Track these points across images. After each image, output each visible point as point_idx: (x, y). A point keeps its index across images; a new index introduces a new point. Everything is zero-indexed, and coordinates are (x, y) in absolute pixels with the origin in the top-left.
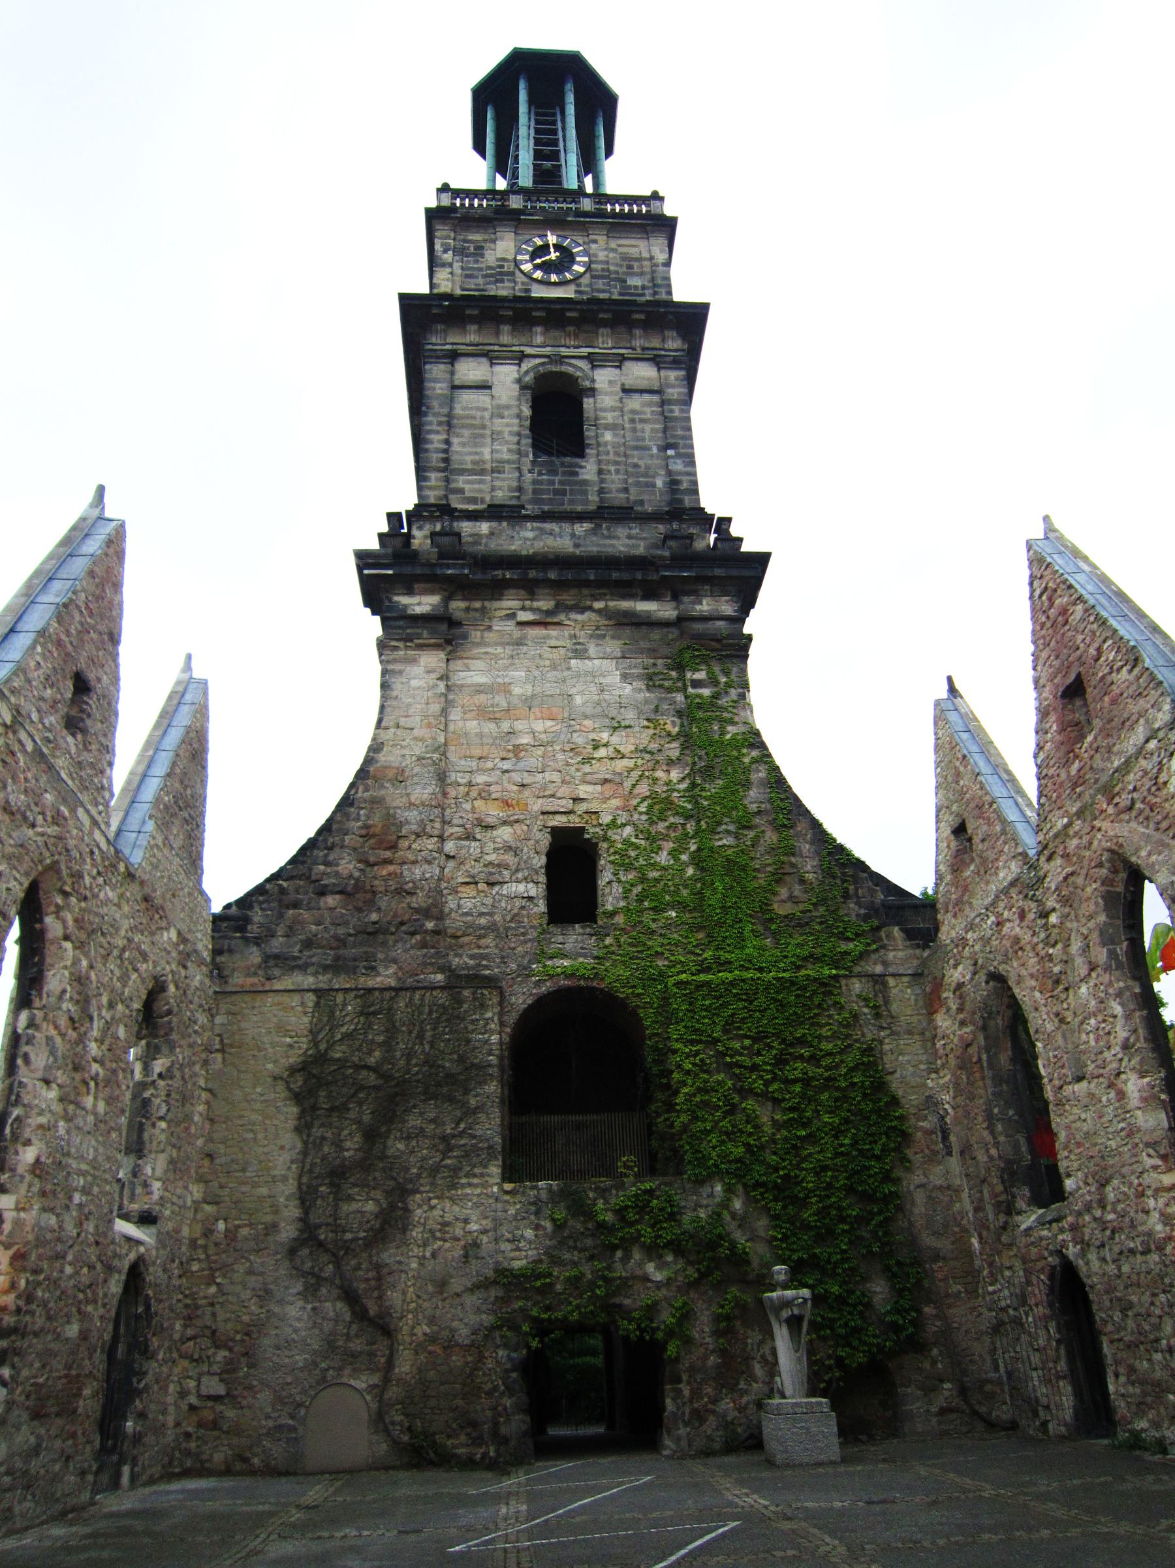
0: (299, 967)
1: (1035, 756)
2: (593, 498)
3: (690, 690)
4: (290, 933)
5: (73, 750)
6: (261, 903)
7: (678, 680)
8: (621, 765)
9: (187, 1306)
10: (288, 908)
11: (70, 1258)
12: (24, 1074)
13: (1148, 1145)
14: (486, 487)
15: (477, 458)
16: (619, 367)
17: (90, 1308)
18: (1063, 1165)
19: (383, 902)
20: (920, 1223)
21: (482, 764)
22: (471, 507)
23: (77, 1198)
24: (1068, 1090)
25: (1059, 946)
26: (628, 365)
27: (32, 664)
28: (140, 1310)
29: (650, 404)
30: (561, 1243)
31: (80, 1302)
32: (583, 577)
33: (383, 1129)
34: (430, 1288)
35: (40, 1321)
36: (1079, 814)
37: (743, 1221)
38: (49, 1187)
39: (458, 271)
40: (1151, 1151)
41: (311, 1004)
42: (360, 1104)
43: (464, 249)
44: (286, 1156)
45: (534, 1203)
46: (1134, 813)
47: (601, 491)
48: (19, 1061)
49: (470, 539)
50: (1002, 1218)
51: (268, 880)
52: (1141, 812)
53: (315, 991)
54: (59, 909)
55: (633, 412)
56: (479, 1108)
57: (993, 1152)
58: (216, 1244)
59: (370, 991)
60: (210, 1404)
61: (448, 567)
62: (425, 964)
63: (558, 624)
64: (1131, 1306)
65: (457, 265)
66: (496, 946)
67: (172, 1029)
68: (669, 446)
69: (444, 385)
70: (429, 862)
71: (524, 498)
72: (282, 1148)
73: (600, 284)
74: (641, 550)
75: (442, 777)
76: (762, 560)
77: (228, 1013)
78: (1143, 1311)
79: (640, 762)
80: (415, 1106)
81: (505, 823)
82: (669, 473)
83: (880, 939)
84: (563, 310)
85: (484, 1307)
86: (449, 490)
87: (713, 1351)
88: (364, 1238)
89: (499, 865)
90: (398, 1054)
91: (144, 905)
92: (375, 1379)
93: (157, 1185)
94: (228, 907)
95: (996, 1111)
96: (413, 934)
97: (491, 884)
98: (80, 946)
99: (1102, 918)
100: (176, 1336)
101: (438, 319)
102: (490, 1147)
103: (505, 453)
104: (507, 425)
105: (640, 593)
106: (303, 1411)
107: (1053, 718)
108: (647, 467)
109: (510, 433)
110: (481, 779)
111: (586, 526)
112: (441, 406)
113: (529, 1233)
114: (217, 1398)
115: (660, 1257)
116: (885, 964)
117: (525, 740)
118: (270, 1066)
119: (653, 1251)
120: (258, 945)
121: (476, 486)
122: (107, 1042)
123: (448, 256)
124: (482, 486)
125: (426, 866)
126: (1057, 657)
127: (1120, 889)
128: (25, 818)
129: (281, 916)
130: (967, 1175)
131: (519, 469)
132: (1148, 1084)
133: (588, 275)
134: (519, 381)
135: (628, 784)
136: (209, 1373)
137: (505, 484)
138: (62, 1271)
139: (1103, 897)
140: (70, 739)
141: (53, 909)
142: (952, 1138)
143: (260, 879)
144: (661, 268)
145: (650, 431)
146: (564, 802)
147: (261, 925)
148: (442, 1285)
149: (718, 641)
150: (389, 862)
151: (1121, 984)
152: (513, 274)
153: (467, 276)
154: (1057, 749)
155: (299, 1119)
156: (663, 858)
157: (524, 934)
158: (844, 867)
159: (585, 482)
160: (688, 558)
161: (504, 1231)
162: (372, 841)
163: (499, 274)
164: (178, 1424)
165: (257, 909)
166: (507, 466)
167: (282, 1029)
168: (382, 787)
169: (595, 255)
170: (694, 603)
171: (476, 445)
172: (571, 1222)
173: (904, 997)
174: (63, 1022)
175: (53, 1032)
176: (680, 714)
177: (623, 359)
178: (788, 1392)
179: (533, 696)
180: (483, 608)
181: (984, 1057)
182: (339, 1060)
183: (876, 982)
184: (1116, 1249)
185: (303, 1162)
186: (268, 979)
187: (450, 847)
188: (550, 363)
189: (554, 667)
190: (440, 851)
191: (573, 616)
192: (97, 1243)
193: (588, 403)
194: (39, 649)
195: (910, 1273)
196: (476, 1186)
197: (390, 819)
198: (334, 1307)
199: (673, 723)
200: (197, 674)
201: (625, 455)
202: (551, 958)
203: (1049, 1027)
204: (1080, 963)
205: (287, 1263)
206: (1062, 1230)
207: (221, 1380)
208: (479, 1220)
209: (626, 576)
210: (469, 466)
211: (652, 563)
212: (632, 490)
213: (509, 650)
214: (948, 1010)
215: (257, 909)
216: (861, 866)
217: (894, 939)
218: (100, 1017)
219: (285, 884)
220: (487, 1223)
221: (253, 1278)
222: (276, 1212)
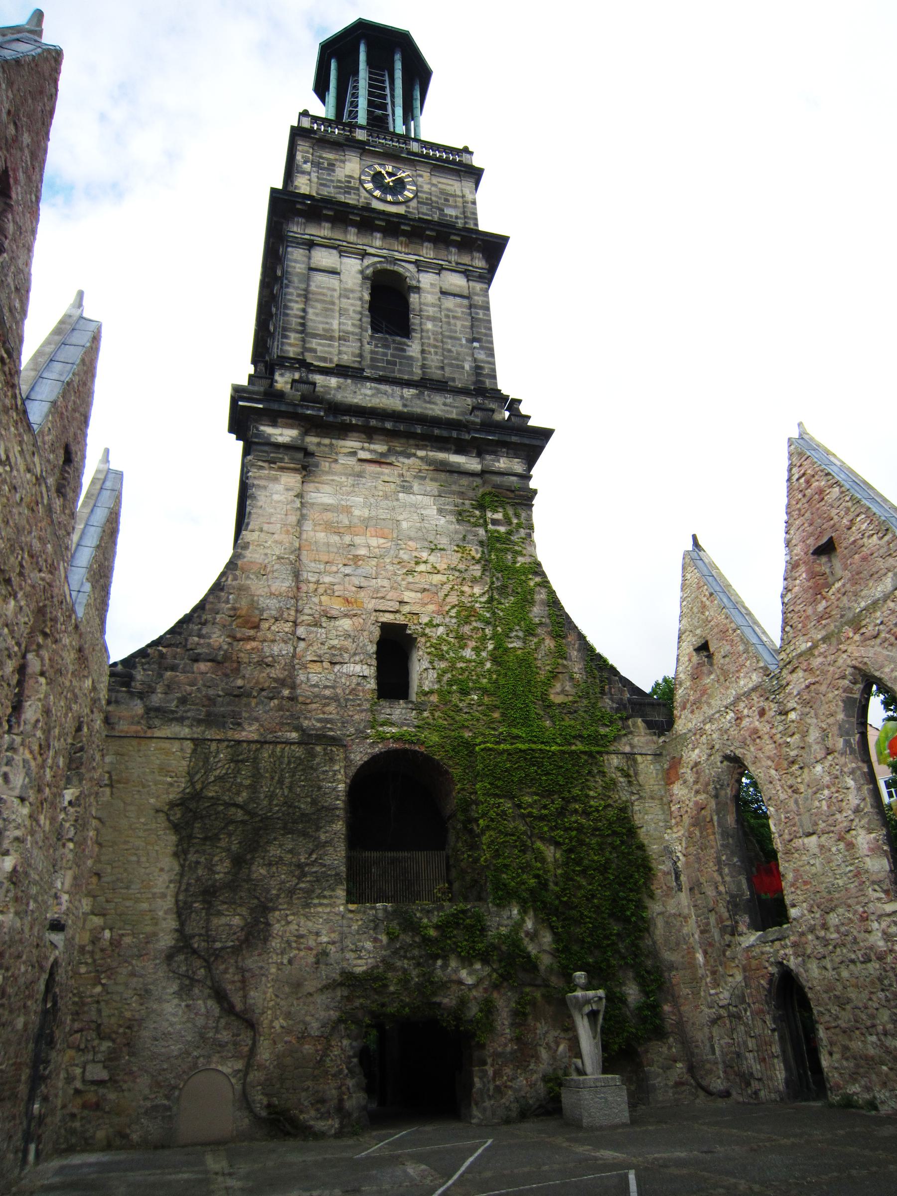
1: (782, 596)
3: (490, 527)
4: (169, 688)
6: (143, 664)
7: (481, 517)
8: (437, 579)
9: (74, 1003)
10: (166, 669)
13: (874, 883)
14: (335, 351)
15: (327, 326)
16: (439, 274)
18: (788, 899)
19: (247, 671)
20: (660, 940)
21: (328, 568)
24: (798, 843)
25: (796, 736)
26: (445, 274)
29: (461, 306)
30: (395, 952)
32: (412, 430)
33: (249, 856)
34: (287, 989)
36: (824, 639)
37: (533, 936)
39: (315, 180)
40: (876, 887)
41: (189, 751)
42: (230, 835)
43: (319, 163)
44: (165, 877)
45: (373, 921)
46: (878, 641)
47: (423, 366)
50: (727, 937)
51: (149, 646)
52: (886, 640)
53: (192, 739)
54: (39, 646)
55: (448, 310)
56: (328, 843)
57: (722, 888)
58: (102, 950)
59: (239, 742)
61: (308, 408)
62: (282, 724)
63: (390, 464)
64: (849, 1001)
65: (314, 175)
66: (338, 713)
67: (82, 764)
68: (474, 340)
69: (303, 266)
70: (285, 642)
72: (162, 870)
73: (424, 209)
74: (453, 415)
75: (297, 575)
76: (545, 434)
77: (117, 754)
78: (861, 1005)
79: (451, 577)
80: (275, 839)
82: (475, 360)
83: (628, 727)
84: (400, 224)
85: (333, 1005)
87: (511, 1040)
88: (232, 947)
89: (340, 649)
90: (262, 796)
92: (239, 1065)
93: (65, 897)
95: (724, 858)
96: (271, 699)
97: (333, 664)
99: (841, 716)
100: (67, 1029)
101: (300, 213)
102: (337, 874)
104: (352, 305)
105: (453, 448)
106: (177, 1093)
107: (802, 568)
108: (458, 353)
109: (354, 311)
110: (327, 579)
111: (413, 391)
112: (300, 282)
113: (369, 945)
114: (100, 1083)
115: (471, 964)
116: (632, 746)
117: (362, 552)
118: (152, 801)
119: (467, 961)
120: (141, 699)
123: (307, 167)
125: (282, 645)
126: (811, 525)
127: (857, 696)
129: (161, 676)
130: (695, 906)
131: (360, 340)
132: (874, 838)
133: (415, 201)
134: (362, 272)
135: (441, 594)
136: (93, 1061)
137: (350, 350)
139: (843, 701)
141: (34, 647)
142: (683, 878)
143: (143, 645)
144: (470, 205)
145: (461, 326)
146: (392, 603)
147: (143, 683)
148: (297, 985)
149: (513, 491)
150: (253, 639)
151: (854, 765)
152: (358, 189)
153: (321, 185)
154: (805, 591)
155: (177, 846)
156: (468, 653)
157: (359, 705)
158: (600, 669)
159: (411, 358)
160: (490, 426)
161: (348, 942)
162: (239, 620)
164: (64, 1106)
165: (139, 668)
166: (351, 337)
167: (164, 770)
168: (248, 577)
171: (326, 317)
172: (402, 937)
173: (649, 771)
174: (36, 748)
175: (28, 756)
176: (481, 543)
178: (589, 1069)
179: (370, 518)
181: (715, 818)
182: (212, 798)
183: (628, 759)
184: (838, 960)
185: (180, 882)
186: (149, 728)
187: (301, 631)
189: (386, 497)
190: (294, 633)
191: (402, 459)
193: (414, 298)
195: (655, 981)
196: (326, 905)
197: (253, 605)
198: (205, 1005)
199: (477, 550)
200: (113, 466)
201: (442, 342)
202: (382, 725)
203: (783, 796)
204: (818, 751)
205: (165, 967)
206: (784, 947)
207: (105, 1067)
208: (329, 931)
209: (445, 433)
210: (321, 332)
212: (447, 369)
213: (351, 480)
214: (685, 782)
215: (139, 668)
216: (613, 671)
219: (164, 650)
220: (335, 936)
221: (135, 979)
222: (156, 924)
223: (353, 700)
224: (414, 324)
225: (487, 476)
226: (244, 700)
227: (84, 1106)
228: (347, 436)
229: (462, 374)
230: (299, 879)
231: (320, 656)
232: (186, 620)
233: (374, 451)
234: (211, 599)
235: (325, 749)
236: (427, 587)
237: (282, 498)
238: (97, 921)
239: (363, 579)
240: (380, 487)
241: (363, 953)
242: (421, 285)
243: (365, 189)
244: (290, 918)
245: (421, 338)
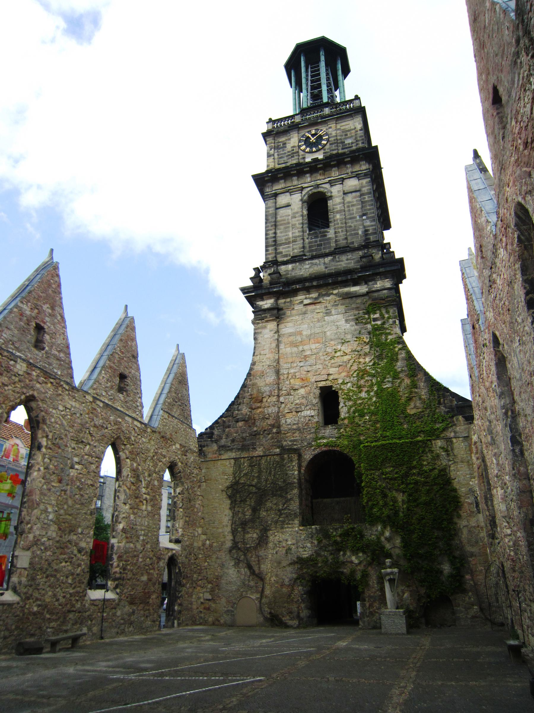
0: (229, 450)
2: (333, 245)
3: (373, 323)
5: (122, 398)
6: (217, 427)
7: (369, 318)
8: (346, 358)
10: (226, 428)
11: (141, 556)
12: (118, 502)
14: (291, 249)
15: (287, 237)
16: (342, 184)
17: (152, 571)
19: (258, 423)
20: (465, 541)
22: (285, 259)
23: (141, 538)
26: (346, 181)
27: (101, 378)
28: (177, 571)
29: (355, 197)
30: (321, 548)
31: (147, 569)
33: (258, 508)
34: (275, 564)
35: (130, 575)
37: (388, 540)
38: (128, 536)
39: (276, 156)
41: (233, 464)
42: (251, 499)
43: (278, 146)
44: (227, 518)
45: (310, 534)
47: (336, 241)
48: (116, 498)
49: (284, 273)
50: (491, 540)
51: (219, 418)
53: (233, 459)
54: (123, 450)
55: (349, 202)
56: (291, 499)
58: (207, 549)
59: (252, 457)
60: (207, 602)
61: (274, 288)
62: (273, 446)
67: (181, 478)
68: (364, 215)
70: (274, 406)
71: (306, 250)
72: (226, 515)
73: (333, 147)
75: (278, 372)
77: (207, 468)
79: (353, 356)
80: (269, 499)
81: (302, 387)
82: (364, 227)
83: (453, 422)
85: (294, 572)
86: (276, 253)
87: (378, 590)
89: (300, 404)
90: (263, 480)
91: (162, 440)
92: (258, 596)
94: (206, 429)
96: (269, 434)
98: (133, 460)
101: (268, 181)
102: (295, 513)
104: (298, 221)
105: (352, 284)
106: (236, 605)
108: (355, 226)
109: (299, 224)
110: (292, 371)
111: (330, 258)
113: (309, 545)
114: (209, 600)
115: (357, 554)
116: (455, 432)
117: (308, 353)
118: (220, 487)
119: (355, 551)
120: (216, 443)
121: (287, 249)
122: (150, 487)
125: (273, 408)
128: (102, 427)
129: (224, 431)
131: (303, 239)
133: (328, 144)
134: (301, 200)
135: (349, 366)
137: (298, 246)
138: (138, 560)
140: (121, 395)
146: (324, 376)
147: (218, 435)
148: (279, 563)
150: (259, 407)
152: (298, 152)
156: (363, 395)
157: (309, 431)
159: (330, 238)
161: (300, 544)
162: (254, 400)
163: (292, 154)
164: (198, 608)
165: (216, 429)
166: (298, 238)
167: (224, 473)
168: (256, 379)
169: (331, 134)
170: (373, 284)
172: (324, 541)
175: (125, 488)
176: (369, 333)
177: (343, 179)
180: (291, 301)
181: (484, 473)
183: (447, 441)
188: (314, 189)
189: (319, 321)
190: (278, 401)
192: (152, 551)
193: (330, 203)
194: (103, 372)
195: (460, 562)
197: (259, 391)
198: (245, 571)
199: (367, 338)
202: (319, 439)
205: (229, 555)
207: (210, 594)
208: (291, 540)
209: (344, 278)
211: (354, 271)
212: (349, 238)
215: (216, 429)
216: (447, 390)
217: (460, 421)
218: (145, 480)
219: (225, 419)
220: (294, 541)
222: (225, 538)
223: (306, 429)
224: (331, 218)
225: (370, 294)
226: (258, 436)
227: (205, 608)
229: (358, 237)
230: (280, 517)
231: (291, 410)
232: (233, 403)
233: (312, 298)
234: (241, 392)
235: (288, 456)
236: (341, 364)
238: (204, 537)
239: (309, 367)
240: (316, 317)
241: (307, 549)
242: (333, 194)
243: (301, 150)
244: (276, 534)
245: (334, 225)
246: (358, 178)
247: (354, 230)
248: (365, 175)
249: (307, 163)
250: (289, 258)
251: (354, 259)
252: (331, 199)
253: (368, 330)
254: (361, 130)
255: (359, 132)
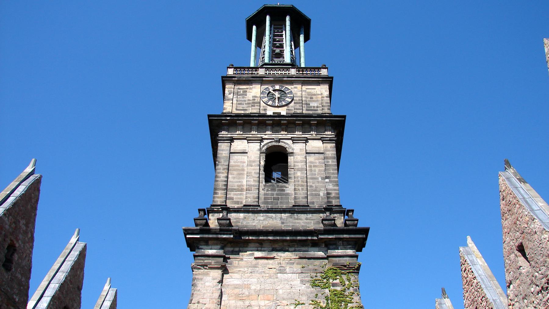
3: (332, 287)
22: (236, 206)
47: (295, 198)
49: (235, 220)
55: (311, 162)
63: (273, 258)
73: (298, 106)
82: (327, 190)
103: (253, 182)
104: (254, 170)
105: (310, 244)
108: (316, 187)
112: (225, 161)
124: (241, 196)
133: (293, 102)
159: (288, 194)
160: (331, 229)
163: (253, 103)
166: (253, 187)
189: (270, 277)
193: (291, 159)
199: (324, 302)
210: (236, 188)
225: (330, 259)
228: (248, 245)
237: (211, 284)
246: (323, 141)
247: (316, 190)
248: (330, 140)
249: (270, 116)
250: (240, 206)
251: (314, 219)
252: (293, 156)
253: (326, 295)
254: (327, 97)
255: (325, 98)
